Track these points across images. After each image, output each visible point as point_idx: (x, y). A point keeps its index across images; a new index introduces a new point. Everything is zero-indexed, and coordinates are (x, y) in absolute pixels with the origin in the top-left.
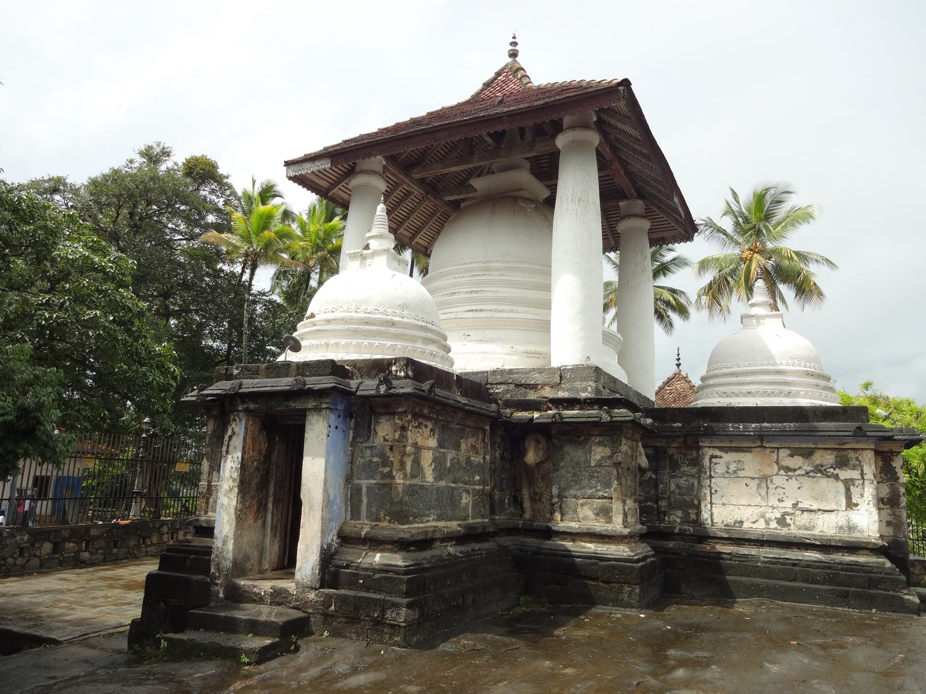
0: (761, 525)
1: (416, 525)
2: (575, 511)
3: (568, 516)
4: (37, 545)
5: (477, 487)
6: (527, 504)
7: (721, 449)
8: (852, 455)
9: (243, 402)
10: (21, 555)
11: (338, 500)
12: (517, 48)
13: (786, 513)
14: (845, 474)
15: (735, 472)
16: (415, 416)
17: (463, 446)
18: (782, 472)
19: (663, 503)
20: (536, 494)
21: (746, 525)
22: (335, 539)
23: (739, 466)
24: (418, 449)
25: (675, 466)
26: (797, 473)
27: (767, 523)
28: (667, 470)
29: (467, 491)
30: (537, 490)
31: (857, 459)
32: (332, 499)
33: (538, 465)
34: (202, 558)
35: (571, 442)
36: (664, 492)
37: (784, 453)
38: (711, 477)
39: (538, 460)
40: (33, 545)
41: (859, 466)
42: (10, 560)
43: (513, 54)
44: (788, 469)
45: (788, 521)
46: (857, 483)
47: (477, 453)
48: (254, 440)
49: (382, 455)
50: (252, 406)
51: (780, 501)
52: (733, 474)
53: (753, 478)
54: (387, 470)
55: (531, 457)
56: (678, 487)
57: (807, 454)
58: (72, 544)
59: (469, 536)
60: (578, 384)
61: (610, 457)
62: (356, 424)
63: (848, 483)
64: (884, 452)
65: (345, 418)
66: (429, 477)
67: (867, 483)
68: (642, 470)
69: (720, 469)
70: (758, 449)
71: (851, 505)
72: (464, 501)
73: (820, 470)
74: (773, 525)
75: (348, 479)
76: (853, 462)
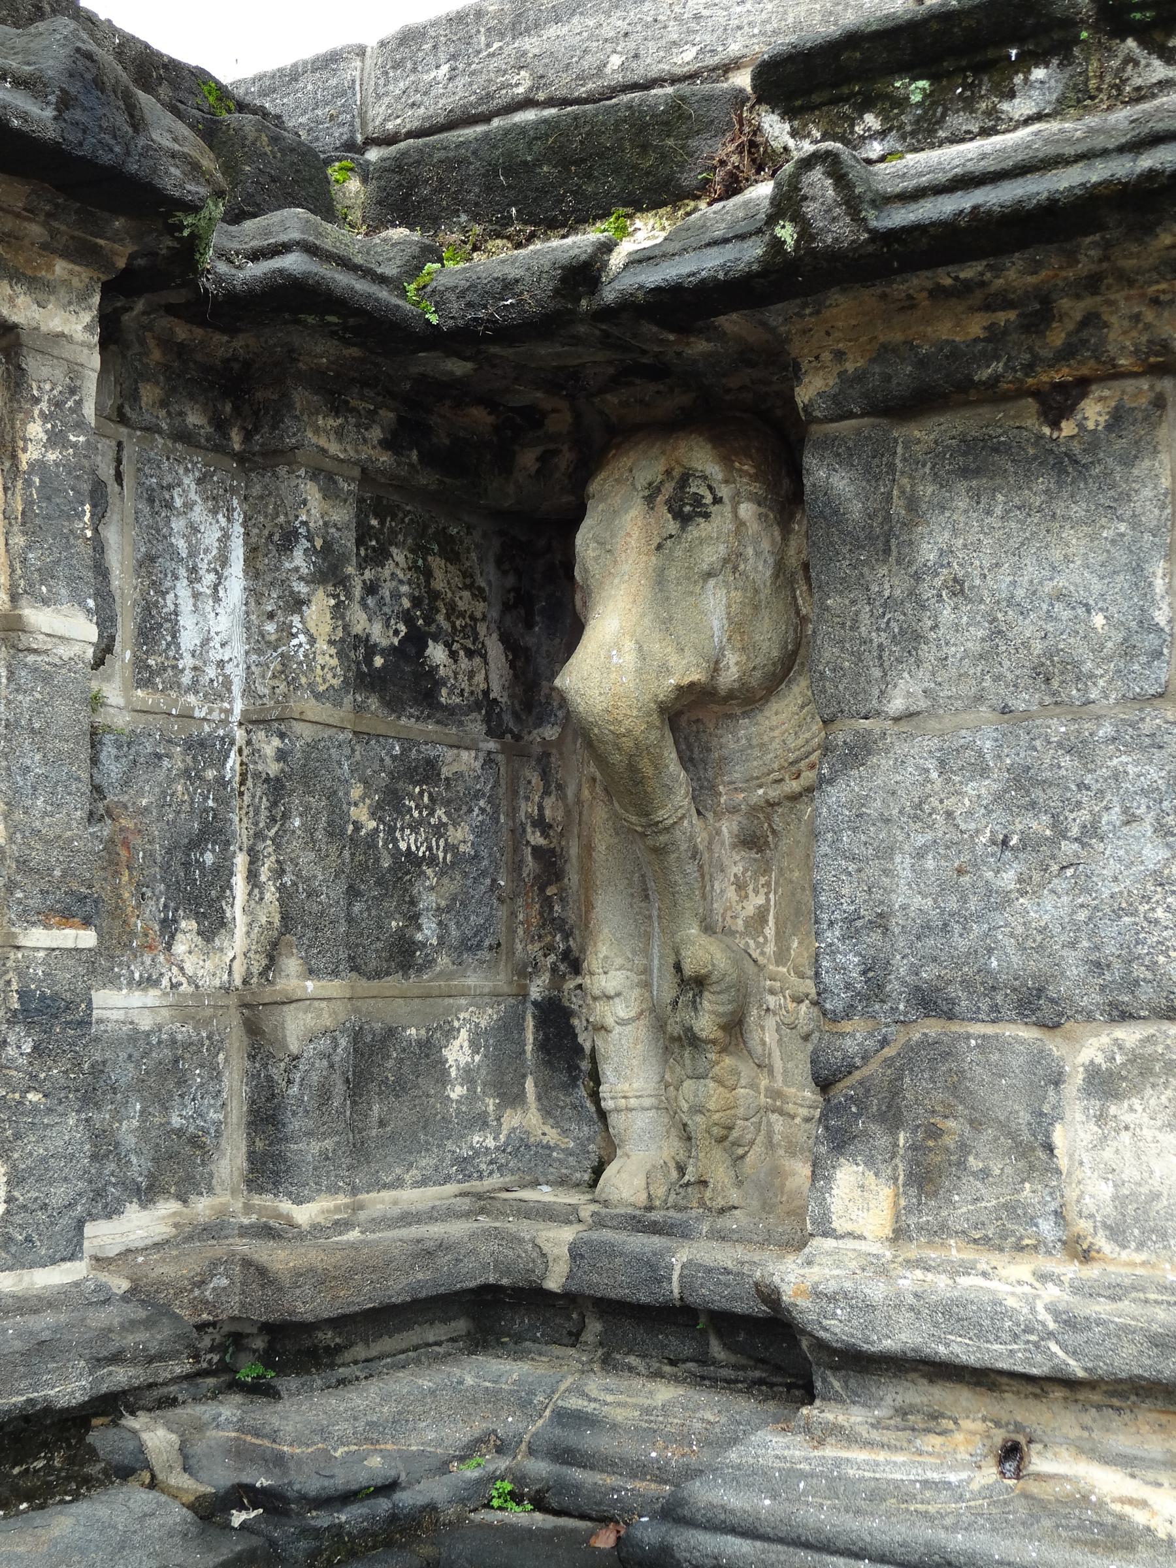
2: (1036, 1152)
3: (966, 1202)
6: (630, 1074)
20: (694, 985)
30: (702, 952)
33: (693, 714)
35: (976, 462)
39: (686, 670)
55: (618, 658)
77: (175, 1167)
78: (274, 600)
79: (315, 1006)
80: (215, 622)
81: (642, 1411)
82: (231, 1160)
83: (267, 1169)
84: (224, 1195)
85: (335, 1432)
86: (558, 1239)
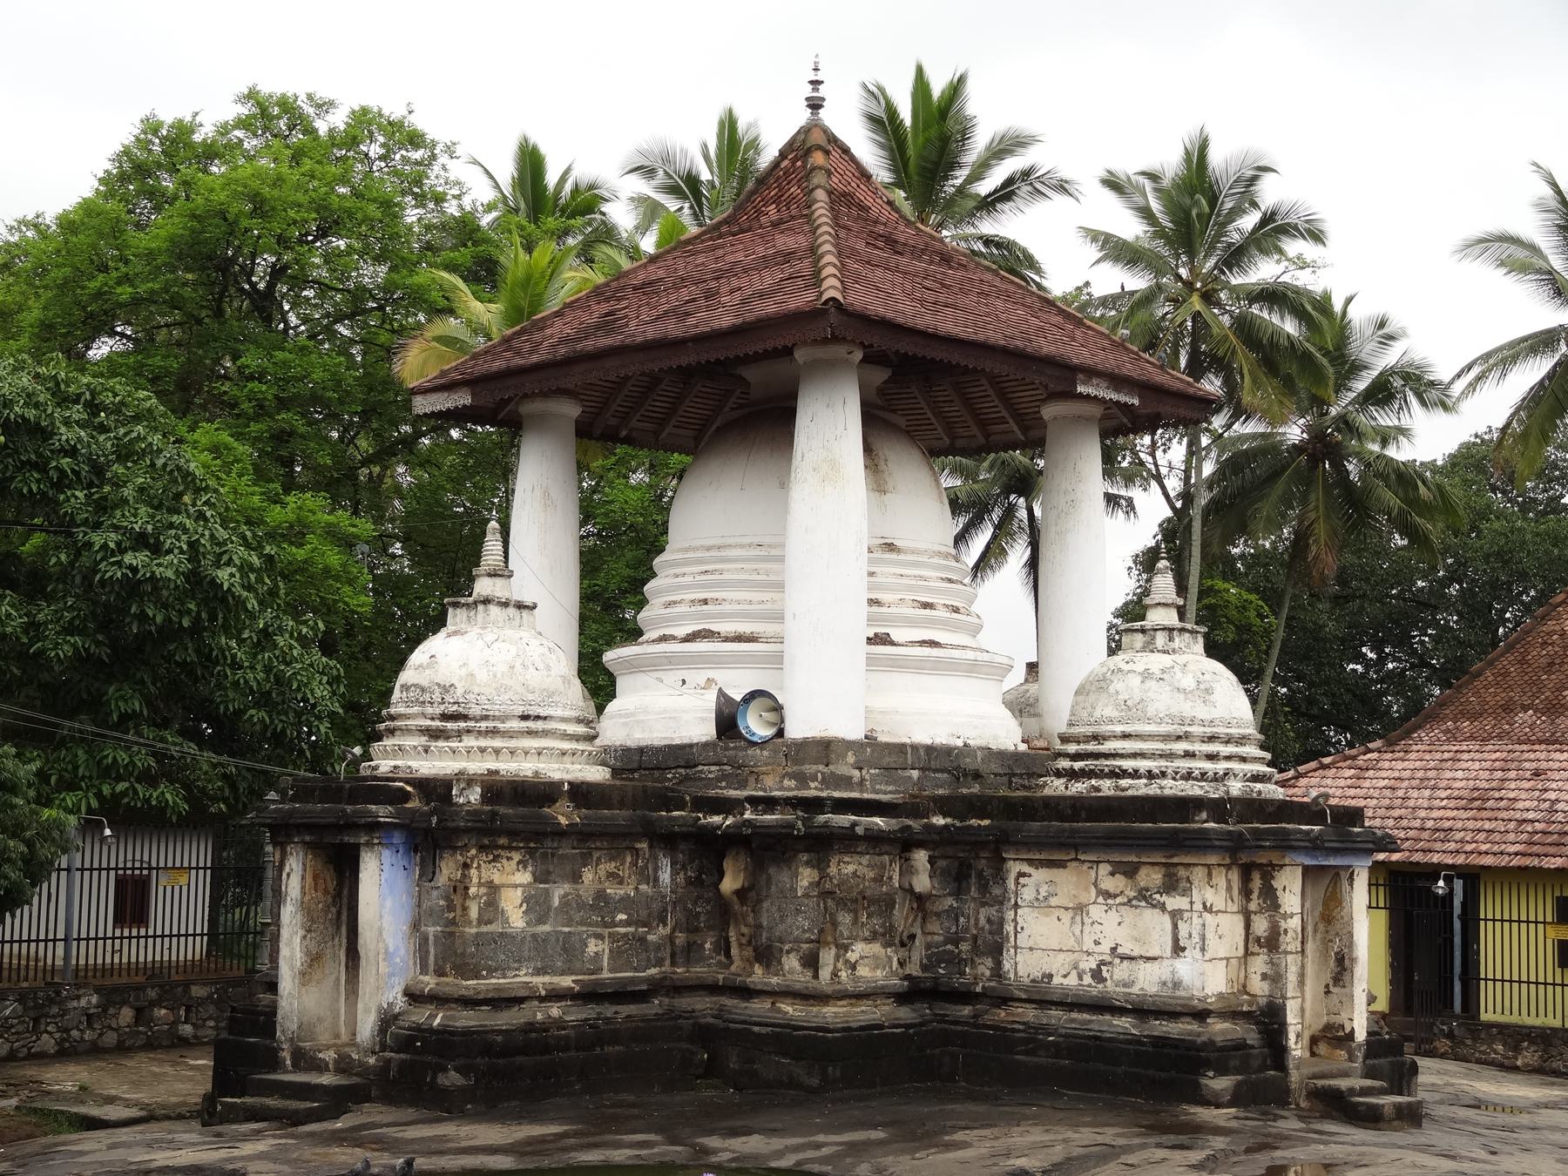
0: (1072, 981)
1: (494, 981)
4: (111, 1011)
5: (622, 930)
6: (734, 951)
7: (1030, 862)
8: (1182, 872)
9: (299, 833)
10: (90, 1026)
11: (402, 952)
12: (823, 91)
13: (1102, 963)
14: (1174, 902)
15: (1046, 898)
16: (482, 848)
17: (588, 875)
18: (1100, 900)
19: (964, 947)
21: (1056, 980)
22: (399, 996)
23: (1051, 890)
25: (984, 888)
26: (1119, 900)
27: (1081, 978)
28: (974, 892)
29: (600, 937)
31: (1189, 881)
32: (391, 949)
34: (266, 1020)
36: (967, 930)
37: (1105, 869)
38: (1016, 906)
40: (105, 1011)
41: (1186, 892)
42: (75, 1033)
43: (815, 105)
44: (1108, 895)
45: (1105, 974)
46: (1186, 915)
47: (621, 883)
48: (315, 877)
49: (447, 898)
50: (307, 838)
51: (1097, 943)
52: (1042, 904)
53: (1067, 909)
54: (452, 915)
55: (729, 884)
56: (989, 921)
57: (1130, 871)
58: (163, 1011)
59: (589, 995)
60: (809, 769)
61: (818, 883)
62: (422, 858)
63: (1176, 915)
64: (1262, 865)
65: (407, 852)
66: (516, 919)
67: (1195, 915)
68: (920, 900)
69: (1027, 894)
70: (1074, 864)
71: (1178, 949)
72: (593, 947)
73: (1143, 895)
74: (1087, 980)
75: (416, 926)
76: (1183, 884)
77: (659, 963)
78: (674, 873)
79: (681, 938)
80: (665, 876)
81: (729, 1002)
82: (668, 962)
83: (673, 964)
84: (667, 968)
85: (685, 1002)
86: (721, 977)
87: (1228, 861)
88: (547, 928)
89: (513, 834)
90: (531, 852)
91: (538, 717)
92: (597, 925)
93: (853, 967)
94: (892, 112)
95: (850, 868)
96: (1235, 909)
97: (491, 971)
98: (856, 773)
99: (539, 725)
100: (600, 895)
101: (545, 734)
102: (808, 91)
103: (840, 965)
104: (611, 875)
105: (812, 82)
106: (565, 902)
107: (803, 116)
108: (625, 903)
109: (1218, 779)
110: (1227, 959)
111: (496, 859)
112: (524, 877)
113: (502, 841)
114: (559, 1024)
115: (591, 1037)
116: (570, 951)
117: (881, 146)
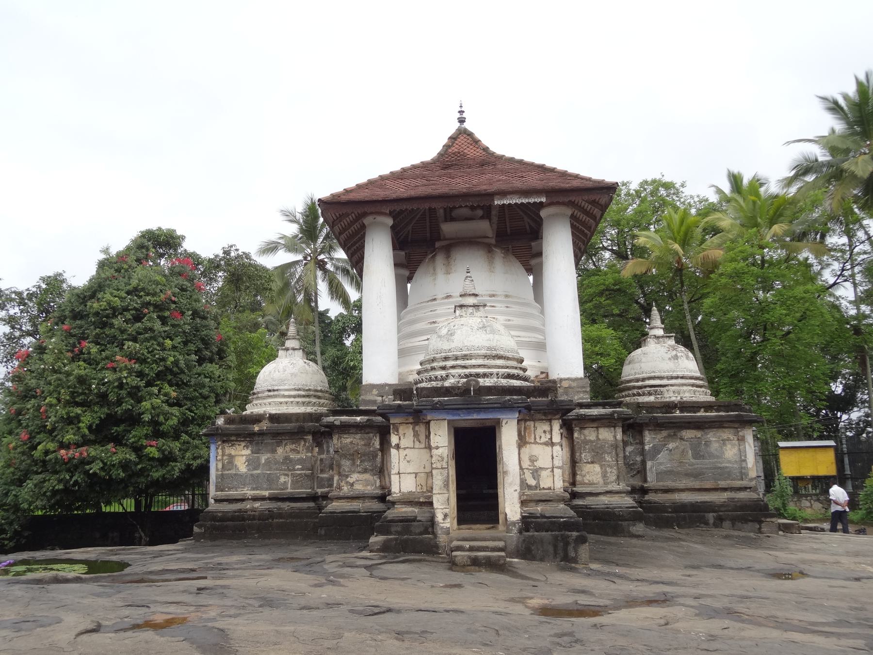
12: (464, 115)
17: (280, 450)
24: (231, 457)
29: (287, 475)
43: (462, 121)
47: (299, 452)
59: (273, 498)
72: (282, 479)
87: (411, 420)
88: (259, 472)
89: (238, 435)
90: (251, 442)
91: (274, 390)
92: (285, 470)
93: (352, 485)
94: (836, 103)
95: (348, 440)
96: (423, 446)
97: (230, 489)
98: (380, 398)
99: (276, 393)
100: (287, 458)
101: (275, 396)
102: (458, 115)
103: (342, 484)
104: (292, 450)
105: (459, 112)
106: (268, 462)
107: (453, 127)
108: (300, 461)
109: (443, 379)
110: (416, 474)
111: (233, 445)
112: (247, 452)
113: (233, 438)
114: (253, 510)
115: (271, 514)
116: (271, 481)
117: (839, 119)
